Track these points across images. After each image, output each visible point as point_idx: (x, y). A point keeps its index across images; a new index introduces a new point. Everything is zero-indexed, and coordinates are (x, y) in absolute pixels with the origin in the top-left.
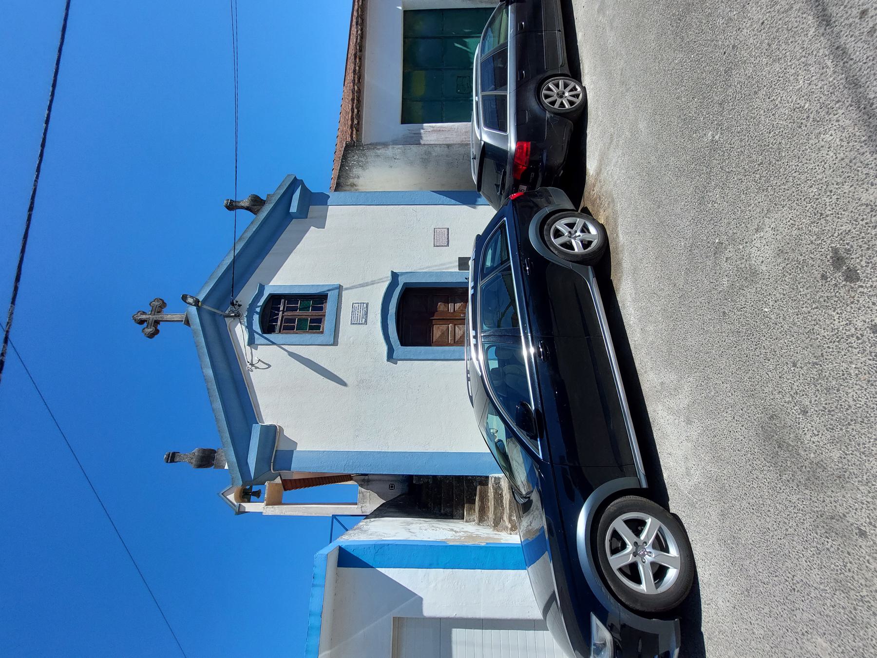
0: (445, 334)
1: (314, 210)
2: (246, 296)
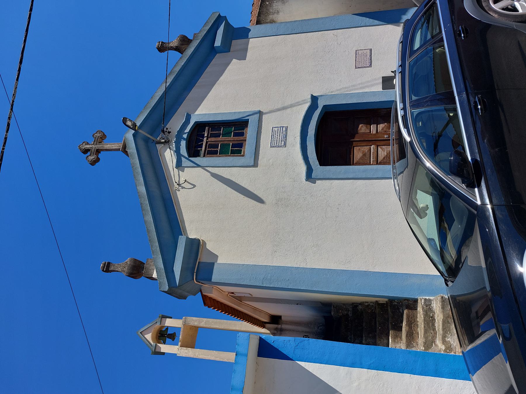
1: (236, 44)
2: (175, 124)
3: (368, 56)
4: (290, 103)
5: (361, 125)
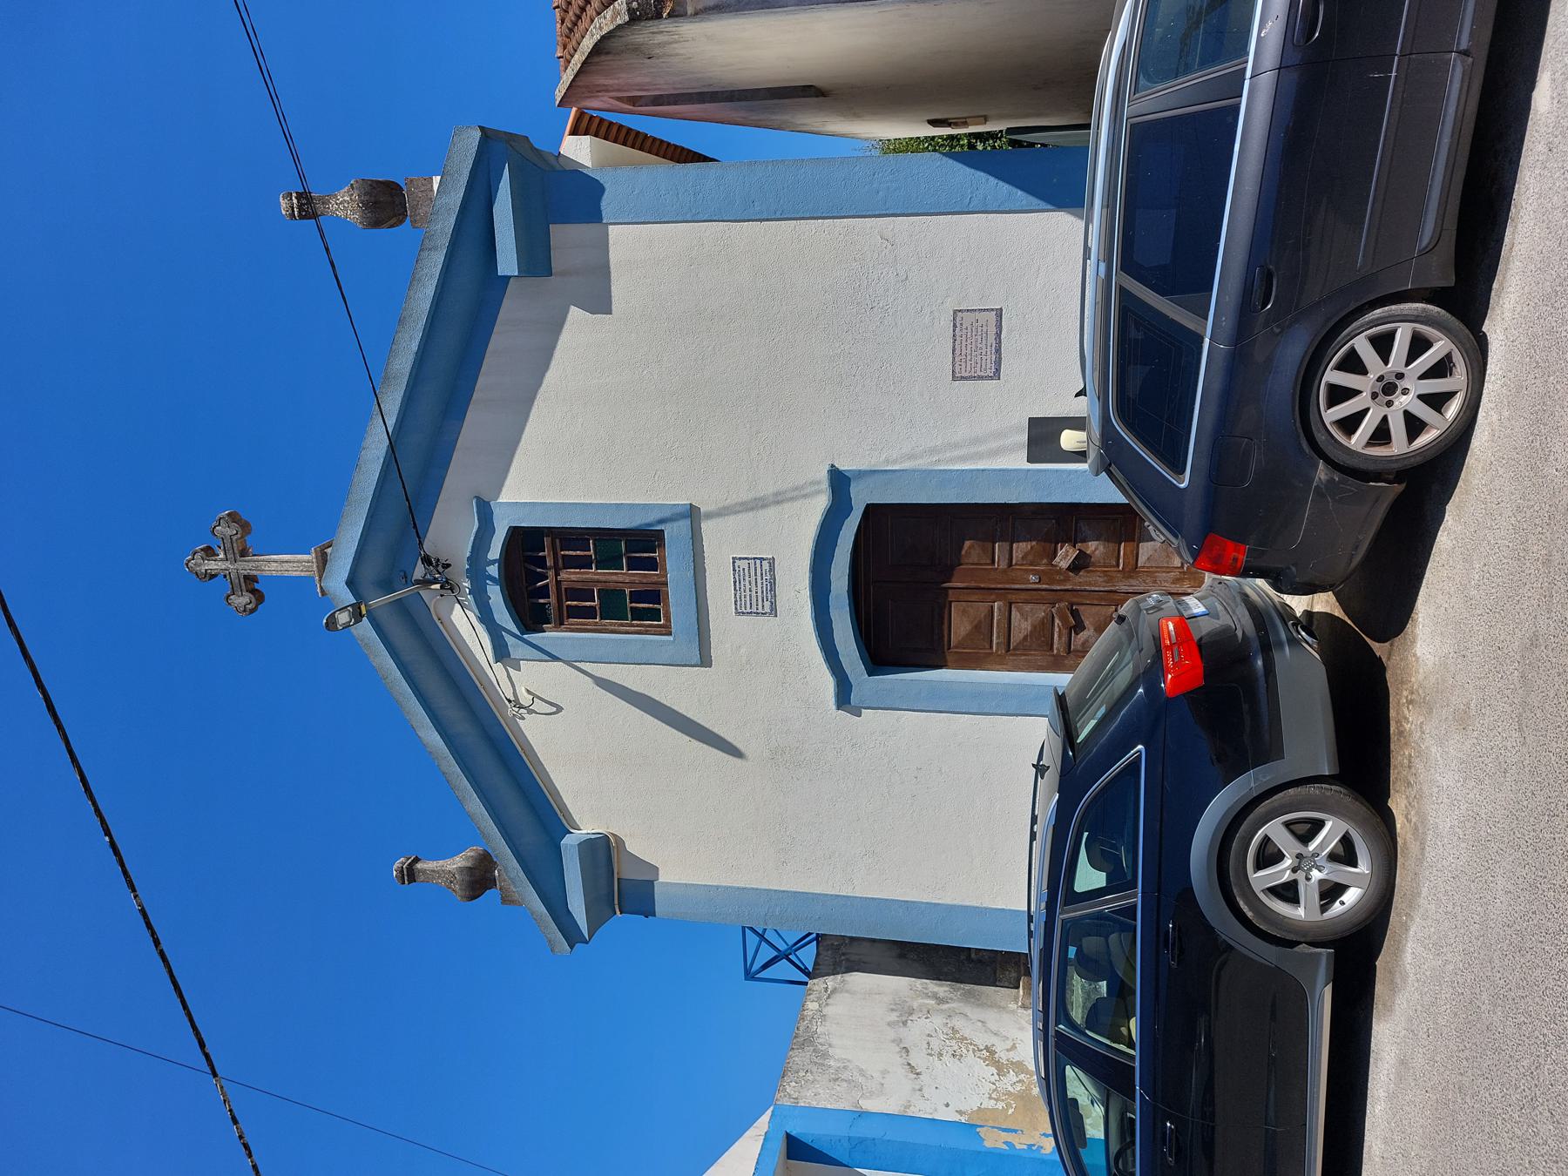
0: (983, 628)
3: (992, 339)
4: (771, 490)
5: (967, 543)
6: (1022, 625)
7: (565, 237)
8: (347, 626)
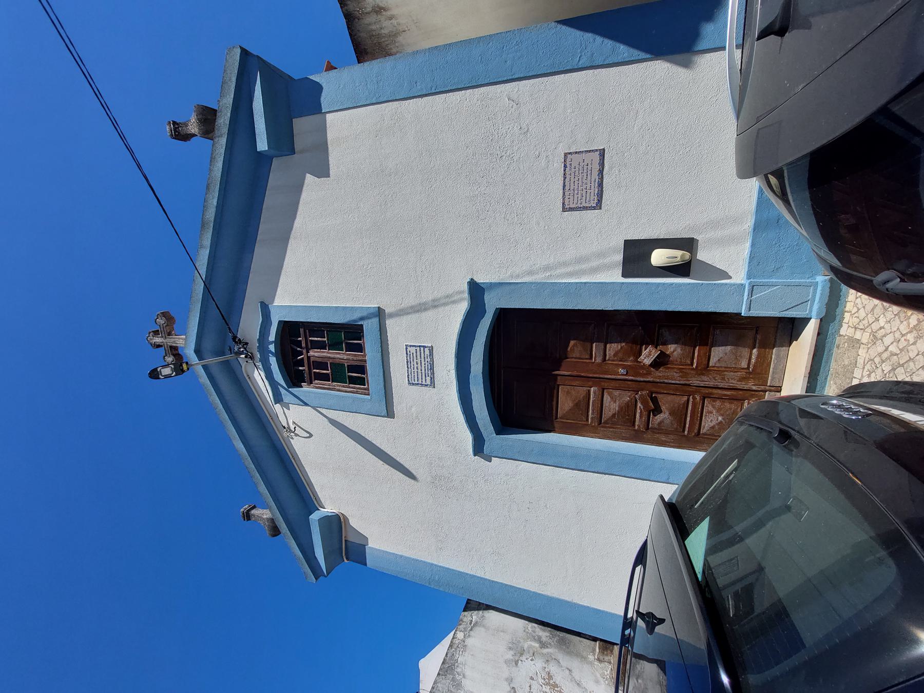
0: (582, 406)
2: (249, 326)
5: (572, 343)
6: (611, 406)
7: (301, 125)
8: (167, 377)
